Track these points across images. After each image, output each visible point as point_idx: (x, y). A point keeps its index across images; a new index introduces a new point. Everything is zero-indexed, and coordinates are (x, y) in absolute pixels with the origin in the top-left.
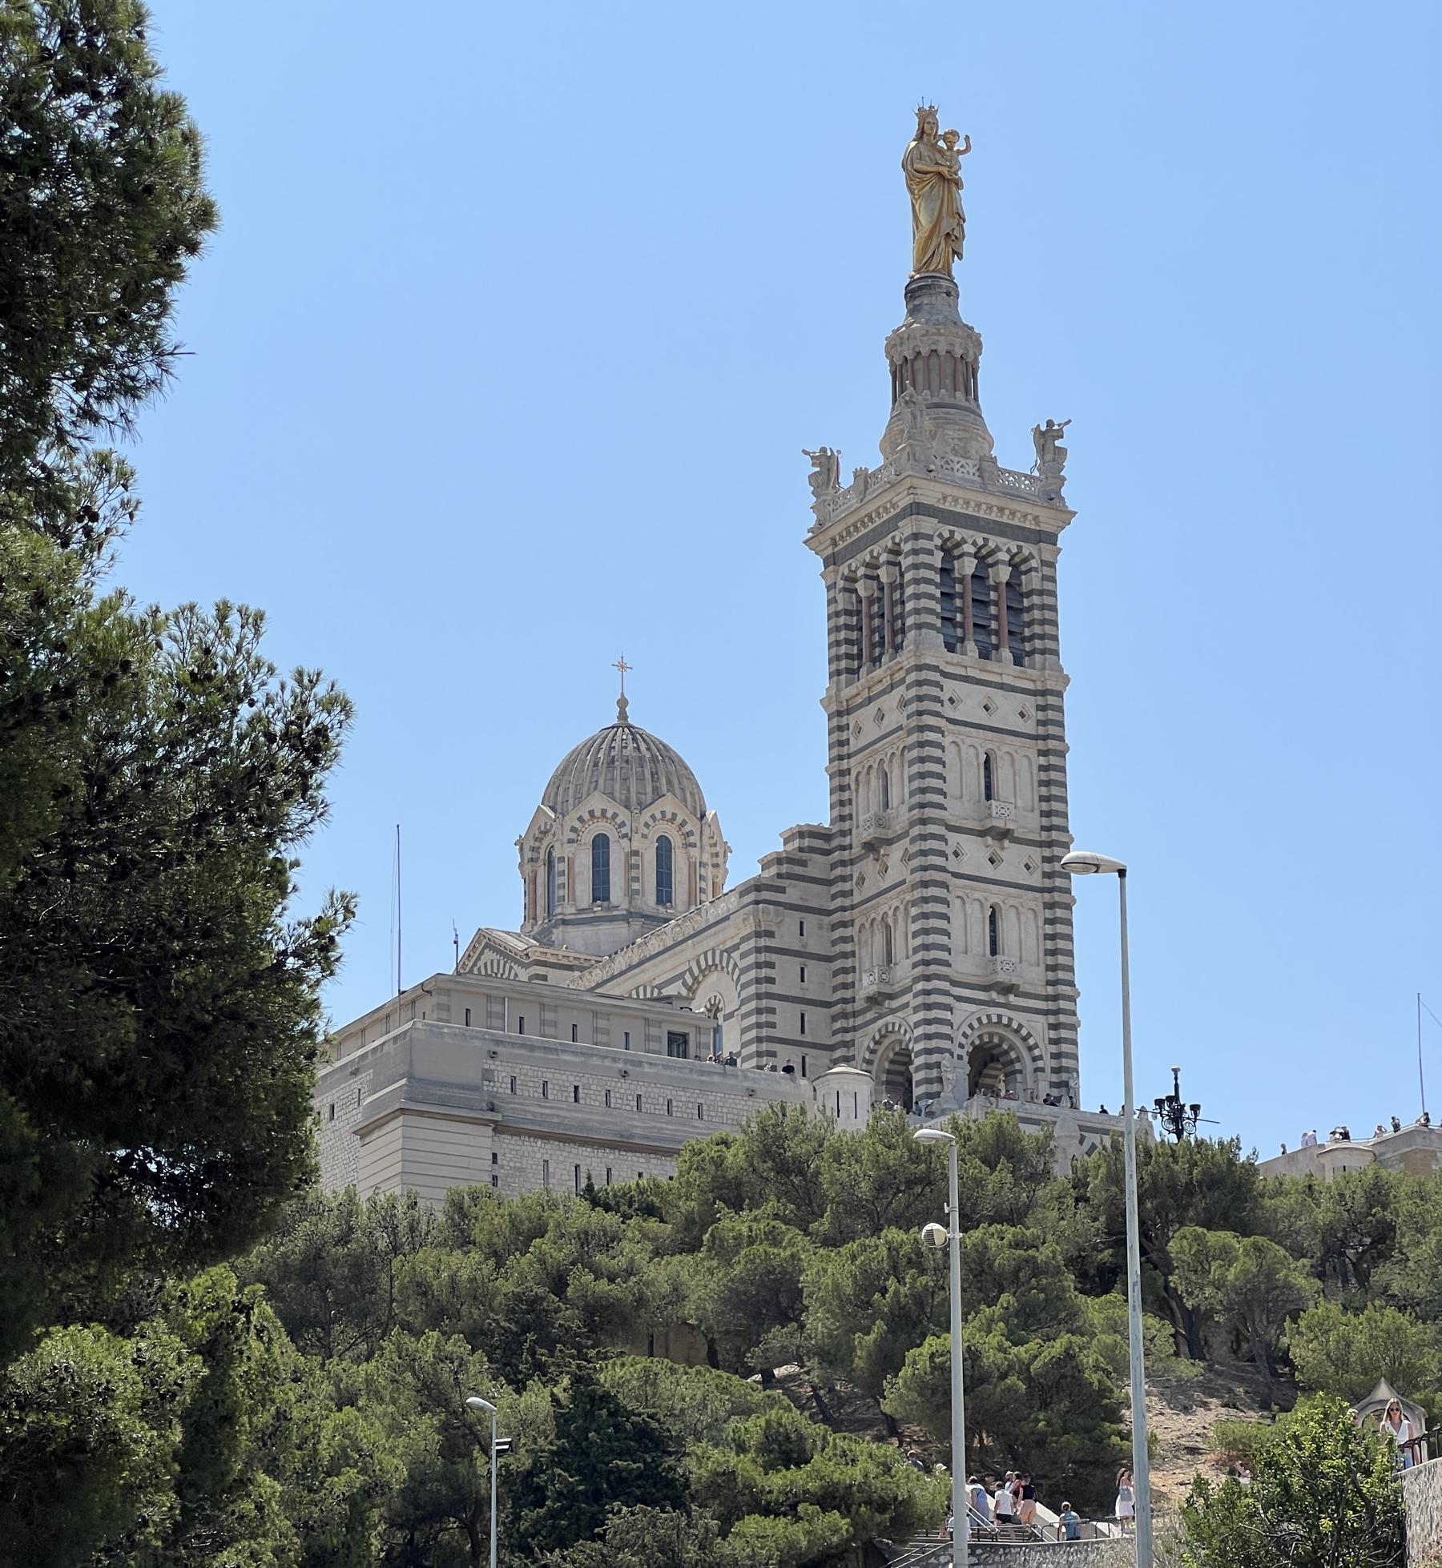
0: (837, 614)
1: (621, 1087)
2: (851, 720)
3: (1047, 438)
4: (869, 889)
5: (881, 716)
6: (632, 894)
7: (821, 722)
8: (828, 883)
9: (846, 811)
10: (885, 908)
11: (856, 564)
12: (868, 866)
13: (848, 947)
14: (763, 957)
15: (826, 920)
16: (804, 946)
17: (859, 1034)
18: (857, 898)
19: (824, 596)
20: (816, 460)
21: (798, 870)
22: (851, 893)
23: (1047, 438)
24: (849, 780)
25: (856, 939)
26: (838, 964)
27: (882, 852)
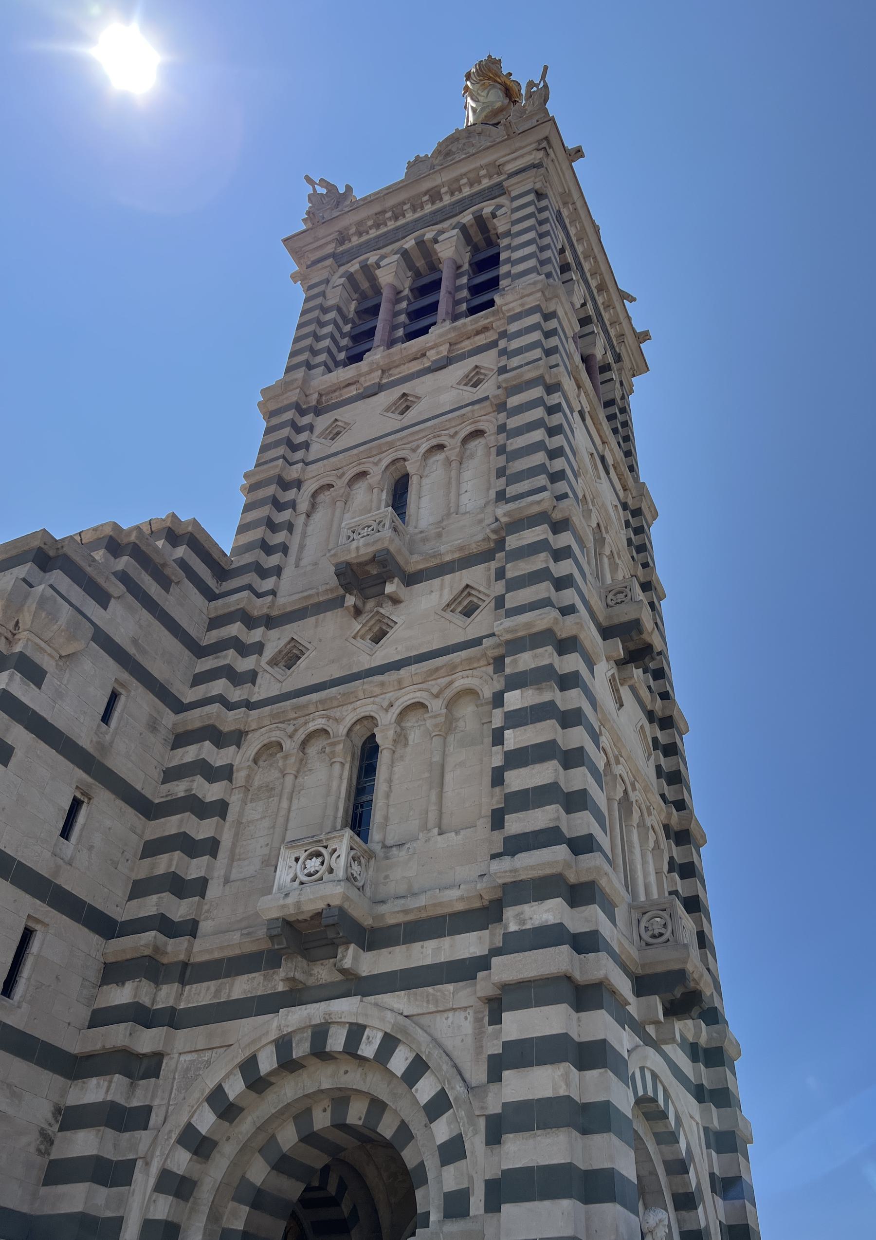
0: (325, 310)
2: (322, 423)
5: (405, 404)
8: (199, 651)
9: (280, 537)
10: (366, 708)
13: (212, 792)
15: (169, 719)
16: (104, 748)
17: (184, 1038)
18: (265, 688)
21: (153, 588)
22: (252, 677)
25: (240, 777)
26: (171, 825)
27: (389, 588)
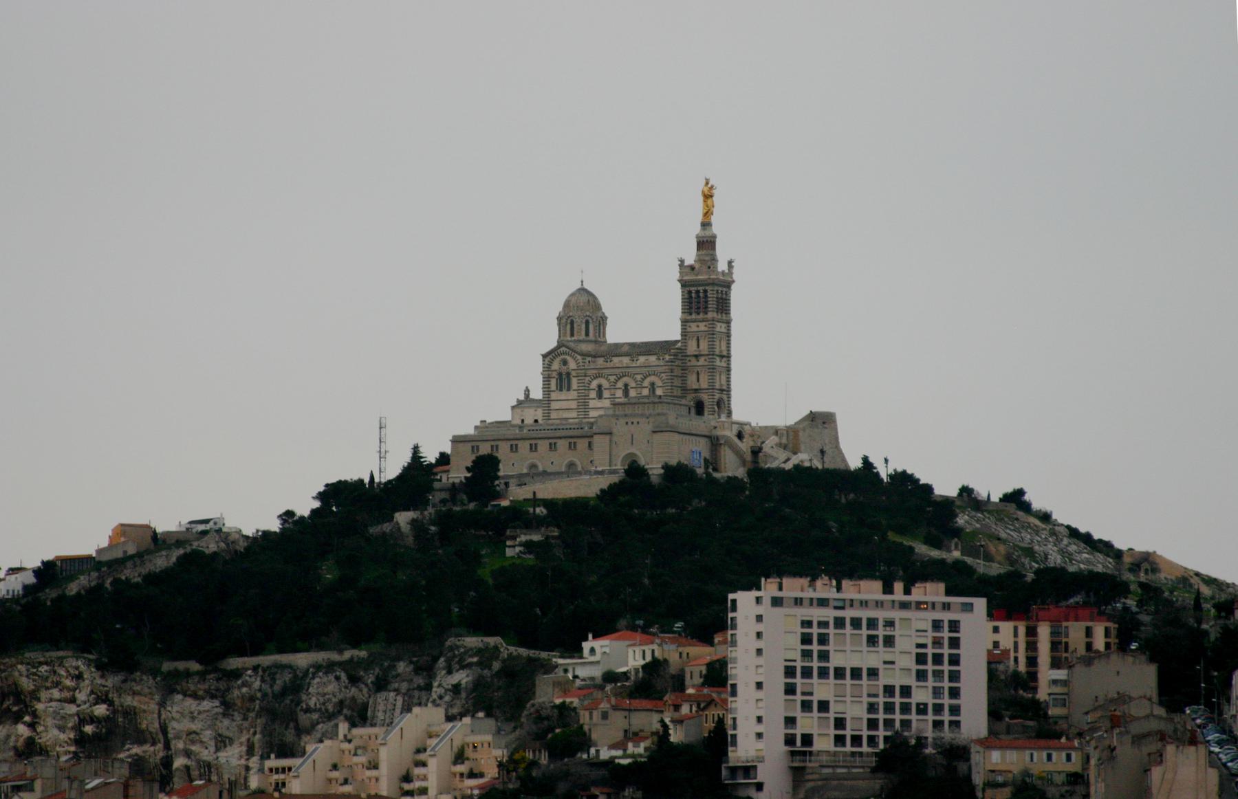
0: (685, 299)
1: (691, 423)
2: (688, 324)
3: (730, 263)
4: (692, 364)
6: (595, 336)
7: (679, 323)
11: (693, 289)
12: (693, 359)
14: (672, 377)
19: (681, 294)
20: (679, 261)
22: (686, 363)
23: (730, 263)
24: (687, 338)
26: (683, 378)
